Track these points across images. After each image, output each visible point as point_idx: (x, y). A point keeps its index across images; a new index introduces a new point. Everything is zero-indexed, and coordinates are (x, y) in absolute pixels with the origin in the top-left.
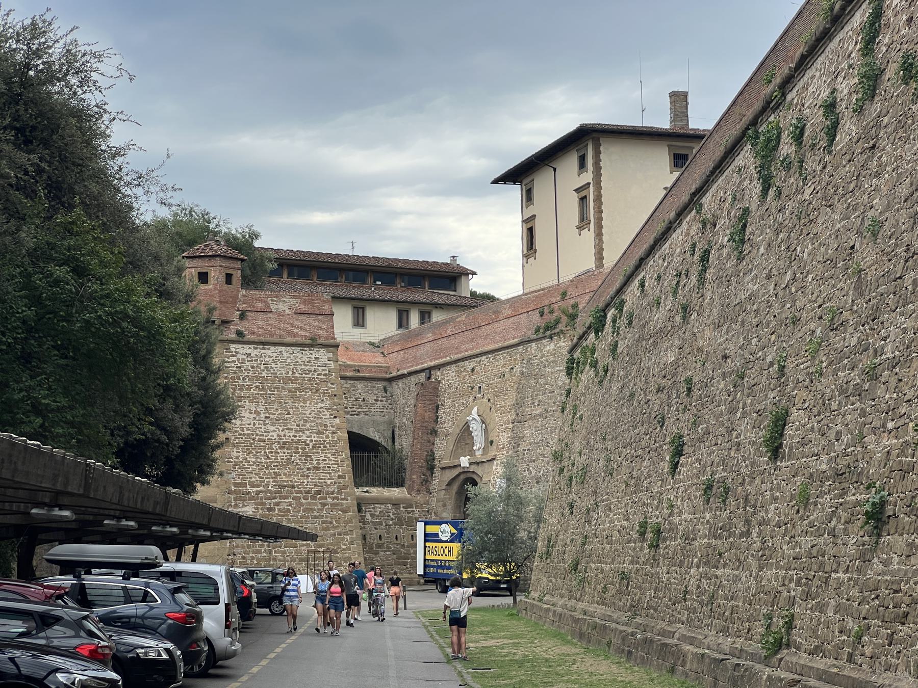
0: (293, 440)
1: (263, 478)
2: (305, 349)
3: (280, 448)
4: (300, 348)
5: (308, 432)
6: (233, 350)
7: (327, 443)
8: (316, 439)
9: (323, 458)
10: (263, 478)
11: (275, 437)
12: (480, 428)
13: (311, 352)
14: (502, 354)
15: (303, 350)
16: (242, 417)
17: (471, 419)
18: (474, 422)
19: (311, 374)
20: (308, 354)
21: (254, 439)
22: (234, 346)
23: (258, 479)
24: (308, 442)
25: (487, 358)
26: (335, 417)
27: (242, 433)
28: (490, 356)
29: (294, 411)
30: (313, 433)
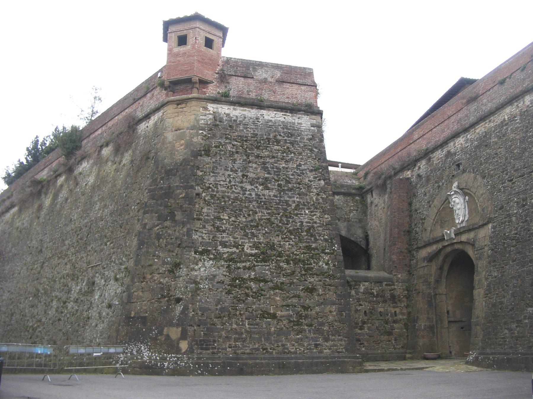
0: (273, 199)
1: (237, 238)
2: (288, 114)
3: (258, 207)
4: (282, 113)
5: (290, 193)
6: (211, 109)
7: (311, 205)
8: (298, 200)
9: (306, 220)
10: (237, 238)
11: (254, 196)
12: (462, 201)
13: (294, 118)
14: (482, 126)
15: (285, 115)
16: (216, 173)
17: (453, 193)
18: (455, 196)
19: (293, 138)
20: (290, 118)
21: (228, 197)
22: (212, 105)
23: (232, 239)
24: (290, 203)
25: (463, 138)
26: (319, 180)
27: (216, 189)
28: (467, 134)
29: (275, 172)
30: (296, 194)
